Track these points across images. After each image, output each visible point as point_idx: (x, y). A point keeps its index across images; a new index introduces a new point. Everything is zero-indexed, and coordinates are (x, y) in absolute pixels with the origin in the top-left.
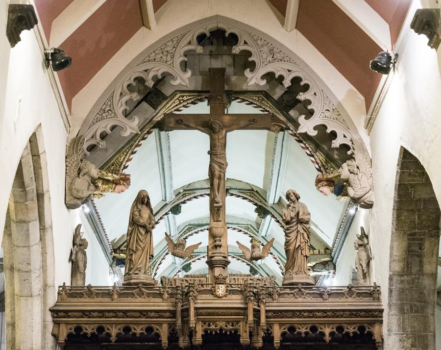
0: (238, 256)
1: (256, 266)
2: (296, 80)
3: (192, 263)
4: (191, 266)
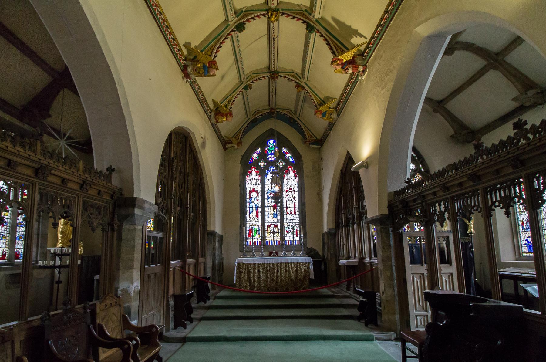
0: (294, 13)
1: (312, 22)
3: (247, 23)
4: (245, 26)
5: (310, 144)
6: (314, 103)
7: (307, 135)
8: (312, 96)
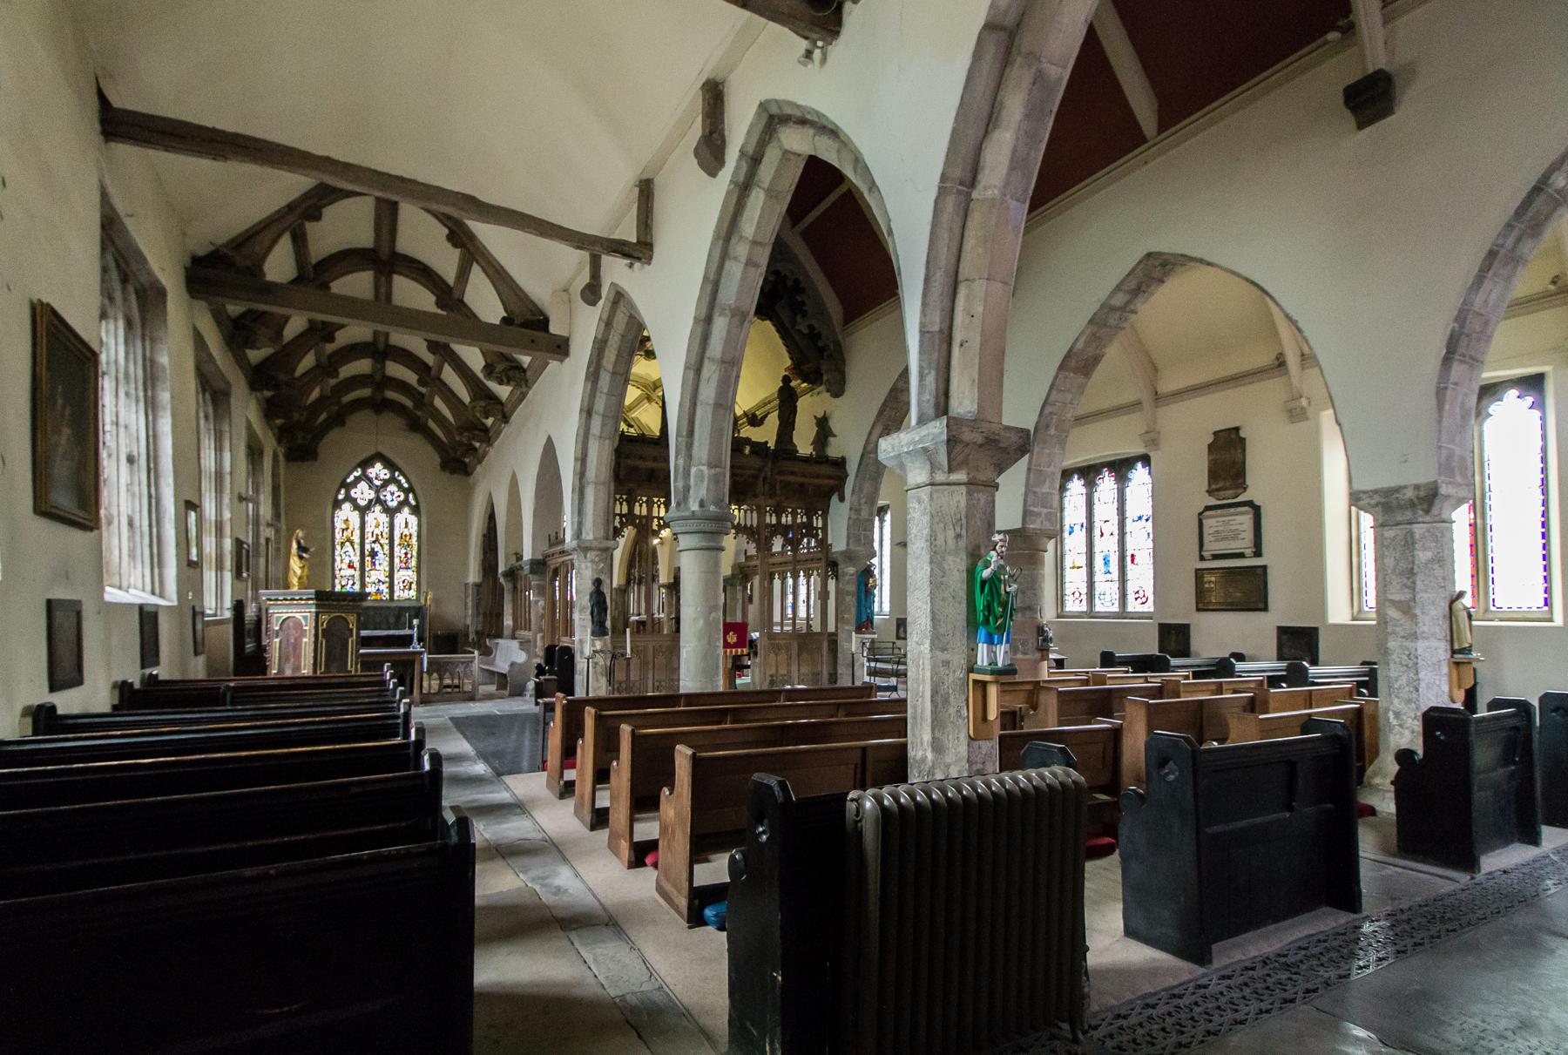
2: (796, 282)
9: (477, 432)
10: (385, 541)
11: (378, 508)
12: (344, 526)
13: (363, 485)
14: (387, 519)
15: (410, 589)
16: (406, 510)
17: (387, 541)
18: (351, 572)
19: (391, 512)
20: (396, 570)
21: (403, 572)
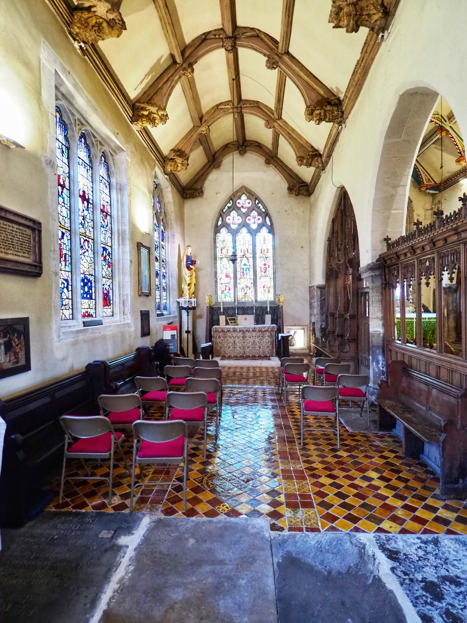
5: (427, 189)
6: (459, 149)
7: (424, 179)
8: (457, 142)
9: (328, 108)
10: (250, 255)
11: (244, 230)
12: (222, 246)
13: (234, 213)
14: (251, 238)
15: (269, 291)
16: (264, 230)
17: (252, 256)
18: (228, 280)
19: (253, 233)
20: (258, 278)
21: (264, 279)
